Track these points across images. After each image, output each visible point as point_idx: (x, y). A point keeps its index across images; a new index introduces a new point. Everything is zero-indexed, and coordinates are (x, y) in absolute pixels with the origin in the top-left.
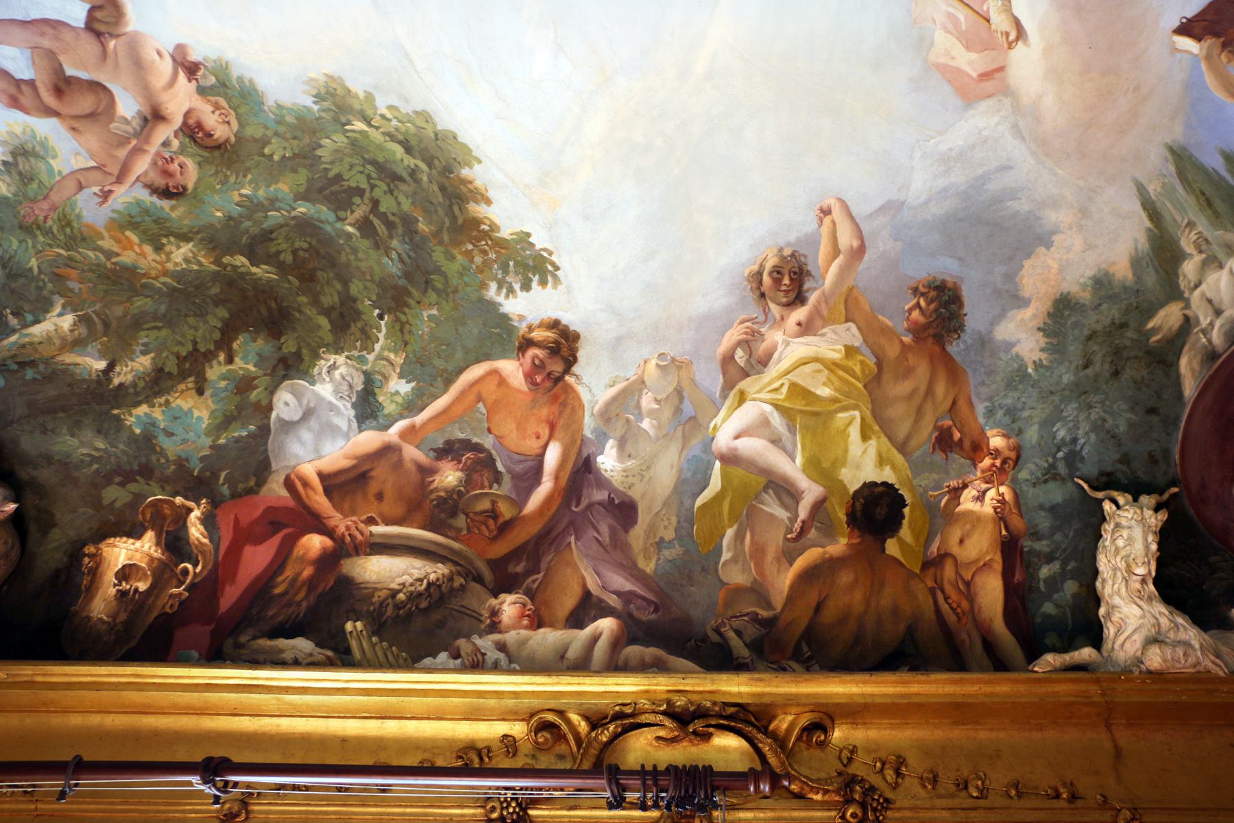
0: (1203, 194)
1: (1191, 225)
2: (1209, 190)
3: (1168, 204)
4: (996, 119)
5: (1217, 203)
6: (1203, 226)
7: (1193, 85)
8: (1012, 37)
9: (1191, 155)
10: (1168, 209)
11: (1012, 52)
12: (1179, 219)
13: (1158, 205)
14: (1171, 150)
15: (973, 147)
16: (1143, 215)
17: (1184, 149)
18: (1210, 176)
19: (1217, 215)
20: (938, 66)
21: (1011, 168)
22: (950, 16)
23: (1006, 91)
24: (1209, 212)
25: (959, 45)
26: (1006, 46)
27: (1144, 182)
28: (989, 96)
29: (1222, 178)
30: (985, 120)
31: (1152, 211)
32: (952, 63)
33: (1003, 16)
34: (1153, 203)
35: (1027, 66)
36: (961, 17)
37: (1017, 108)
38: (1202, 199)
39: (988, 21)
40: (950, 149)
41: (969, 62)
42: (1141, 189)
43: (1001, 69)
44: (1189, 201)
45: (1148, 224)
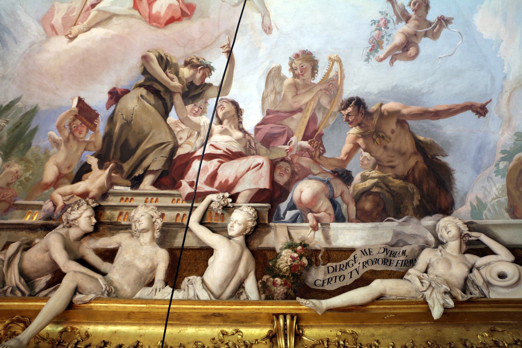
0: (21, 124)
1: (7, 122)
2: (22, 126)
3: (14, 112)
4: (36, 34)
5: (18, 130)
6: (8, 127)
7: (61, 109)
8: (70, 36)
9: (34, 115)
10: (12, 112)
11: (64, 37)
12: (8, 117)
13: (13, 108)
14: (36, 107)
15: (22, 25)
16: (8, 103)
17: (37, 112)
18: (28, 125)
19: (13, 131)
20: (53, 6)
21: (16, 44)
22: (75, 9)
23: (48, 37)
24: (14, 128)
25: (63, 14)
26: (66, 34)
27: (22, 100)
28: (45, 30)
29: (28, 129)
30: (35, 30)
31: (11, 105)
32: (56, 12)
33: (77, 31)
34: (13, 105)
35: (59, 44)
36: (74, 14)
37: (42, 43)
38: (18, 124)
39: (75, 25)
40: (19, 16)
41: (57, 20)
42: (18, 99)
43: (57, 34)
44: (17, 119)
45: (4, 105)
